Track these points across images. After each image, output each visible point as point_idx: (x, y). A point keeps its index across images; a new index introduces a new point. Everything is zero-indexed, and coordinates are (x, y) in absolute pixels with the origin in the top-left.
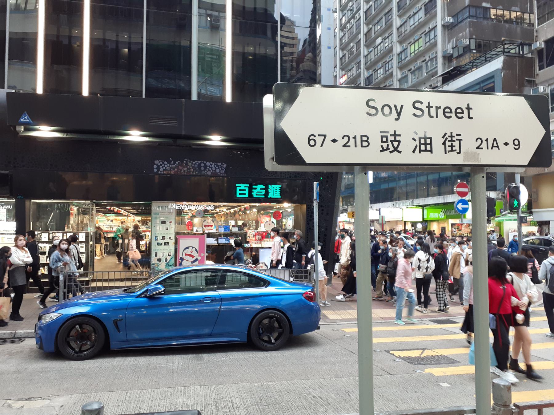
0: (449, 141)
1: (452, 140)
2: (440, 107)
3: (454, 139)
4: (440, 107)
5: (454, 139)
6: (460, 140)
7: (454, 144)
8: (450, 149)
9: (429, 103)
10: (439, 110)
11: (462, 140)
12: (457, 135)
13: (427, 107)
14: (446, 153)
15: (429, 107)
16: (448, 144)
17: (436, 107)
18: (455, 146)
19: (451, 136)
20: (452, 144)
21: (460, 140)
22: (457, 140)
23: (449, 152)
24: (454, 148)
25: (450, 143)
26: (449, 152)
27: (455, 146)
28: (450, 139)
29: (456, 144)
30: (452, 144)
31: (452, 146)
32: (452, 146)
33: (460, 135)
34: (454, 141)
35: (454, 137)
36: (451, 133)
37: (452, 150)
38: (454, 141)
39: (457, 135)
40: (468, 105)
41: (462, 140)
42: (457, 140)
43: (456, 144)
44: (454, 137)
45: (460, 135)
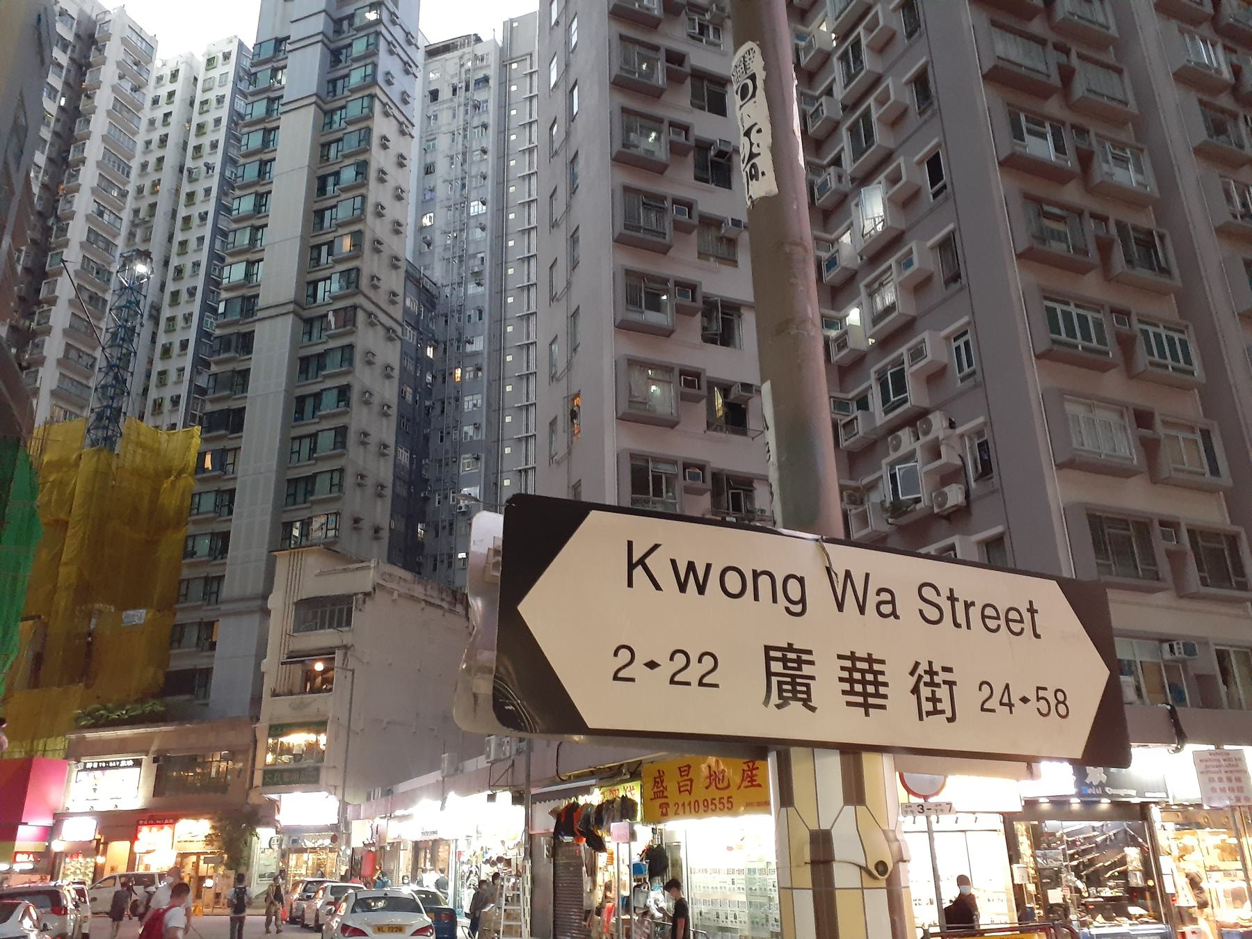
0: (926, 684)
1: (931, 684)
2: (973, 604)
3: (937, 679)
4: (973, 604)
5: (937, 679)
6: (951, 684)
9: (951, 590)
10: (972, 609)
13: (948, 598)
15: (952, 599)
17: (966, 602)
22: (945, 682)
25: (929, 689)
34: (938, 685)
38: (938, 685)
40: (1031, 602)
42: (945, 682)
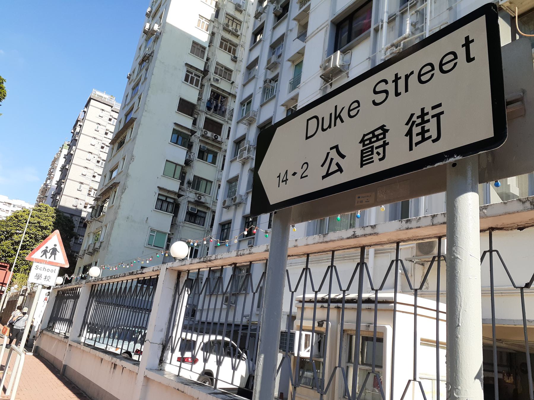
2: (412, 73)
3: (426, 118)
4: (412, 73)
5: (426, 118)
7: (427, 126)
8: (419, 138)
11: (442, 113)
12: (433, 108)
14: (411, 149)
15: (397, 79)
16: (417, 130)
18: (428, 131)
19: (423, 114)
20: (423, 128)
21: (438, 116)
23: (417, 144)
24: (427, 135)
26: (417, 144)
27: (428, 131)
28: (419, 121)
29: (432, 126)
30: (423, 128)
31: (423, 132)
32: (423, 132)
33: (440, 105)
34: (428, 121)
35: (427, 114)
36: (423, 110)
37: (424, 140)
38: (428, 121)
39: (433, 108)
41: (442, 113)
43: (432, 126)
44: (427, 114)
45: (440, 105)
